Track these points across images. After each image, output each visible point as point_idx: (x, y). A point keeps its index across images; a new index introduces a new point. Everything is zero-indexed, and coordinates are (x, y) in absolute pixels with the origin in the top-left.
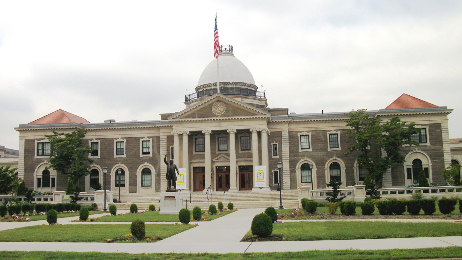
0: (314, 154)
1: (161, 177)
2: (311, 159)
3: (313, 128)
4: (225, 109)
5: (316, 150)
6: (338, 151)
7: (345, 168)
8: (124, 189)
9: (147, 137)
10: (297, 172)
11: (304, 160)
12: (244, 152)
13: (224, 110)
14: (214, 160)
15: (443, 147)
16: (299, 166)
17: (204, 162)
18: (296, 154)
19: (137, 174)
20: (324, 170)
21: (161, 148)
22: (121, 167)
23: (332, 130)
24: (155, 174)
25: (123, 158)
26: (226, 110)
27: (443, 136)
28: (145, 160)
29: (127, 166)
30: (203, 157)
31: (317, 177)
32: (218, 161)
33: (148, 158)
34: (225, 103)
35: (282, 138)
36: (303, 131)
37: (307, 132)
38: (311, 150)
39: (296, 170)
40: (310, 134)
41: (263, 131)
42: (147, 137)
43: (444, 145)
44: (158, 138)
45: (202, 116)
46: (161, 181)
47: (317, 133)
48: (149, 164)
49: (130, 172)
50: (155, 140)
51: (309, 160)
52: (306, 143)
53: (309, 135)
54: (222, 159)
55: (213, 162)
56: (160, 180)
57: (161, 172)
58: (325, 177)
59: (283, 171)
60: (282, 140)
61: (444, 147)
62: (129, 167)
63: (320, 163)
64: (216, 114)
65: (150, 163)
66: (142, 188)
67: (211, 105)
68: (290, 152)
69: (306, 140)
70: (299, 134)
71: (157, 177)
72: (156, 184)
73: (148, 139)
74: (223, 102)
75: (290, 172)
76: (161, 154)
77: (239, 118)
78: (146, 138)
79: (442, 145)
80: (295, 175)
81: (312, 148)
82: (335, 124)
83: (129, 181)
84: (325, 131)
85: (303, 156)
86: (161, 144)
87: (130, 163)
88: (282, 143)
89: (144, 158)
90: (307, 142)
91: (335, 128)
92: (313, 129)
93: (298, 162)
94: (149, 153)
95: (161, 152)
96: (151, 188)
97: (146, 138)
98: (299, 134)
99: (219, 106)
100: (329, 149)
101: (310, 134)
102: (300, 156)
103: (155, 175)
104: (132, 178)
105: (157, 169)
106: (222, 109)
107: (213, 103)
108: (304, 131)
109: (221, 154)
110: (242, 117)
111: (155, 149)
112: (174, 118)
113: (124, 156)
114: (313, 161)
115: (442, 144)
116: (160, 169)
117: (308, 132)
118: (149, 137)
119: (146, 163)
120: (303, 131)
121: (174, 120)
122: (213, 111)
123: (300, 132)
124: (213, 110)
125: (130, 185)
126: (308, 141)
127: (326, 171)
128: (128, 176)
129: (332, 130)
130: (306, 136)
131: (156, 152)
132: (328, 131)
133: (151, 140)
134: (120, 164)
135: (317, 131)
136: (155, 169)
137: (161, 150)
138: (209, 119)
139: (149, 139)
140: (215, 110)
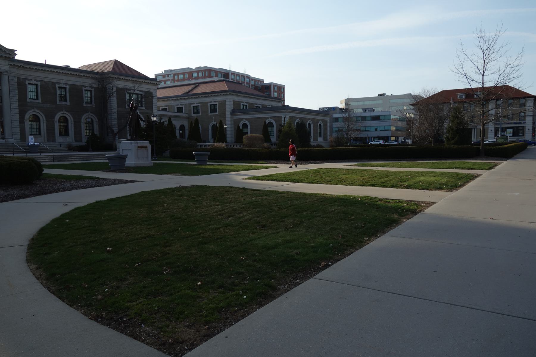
3: (42, 78)
6: (66, 105)
7: (74, 123)
15: (153, 112)
16: (27, 116)
20: (54, 124)
23: (61, 83)
27: (154, 103)
31: (47, 130)
36: (32, 80)
38: (40, 101)
39: (25, 121)
40: (39, 84)
43: (154, 110)
51: (38, 112)
52: (33, 93)
58: (54, 130)
61: (154, 112)
63: (50, 117)
69: (33, 89)
70: (27, 82)
75: (20, 123)
79: (153, 110)
81: (41, 99)
82: (64, 77)
84: (54, 84)
91: (64, 82)
93: (26, 112)
100: (58, 103)
101: (39, 84)
114: (43, 113)
115: (153, 109)
117: (37, 81)
120: (32, 80)
126: (35, 91)
127: (56, 124)
129: (61, 83)
130: (33, 86)
132: (58, 84)
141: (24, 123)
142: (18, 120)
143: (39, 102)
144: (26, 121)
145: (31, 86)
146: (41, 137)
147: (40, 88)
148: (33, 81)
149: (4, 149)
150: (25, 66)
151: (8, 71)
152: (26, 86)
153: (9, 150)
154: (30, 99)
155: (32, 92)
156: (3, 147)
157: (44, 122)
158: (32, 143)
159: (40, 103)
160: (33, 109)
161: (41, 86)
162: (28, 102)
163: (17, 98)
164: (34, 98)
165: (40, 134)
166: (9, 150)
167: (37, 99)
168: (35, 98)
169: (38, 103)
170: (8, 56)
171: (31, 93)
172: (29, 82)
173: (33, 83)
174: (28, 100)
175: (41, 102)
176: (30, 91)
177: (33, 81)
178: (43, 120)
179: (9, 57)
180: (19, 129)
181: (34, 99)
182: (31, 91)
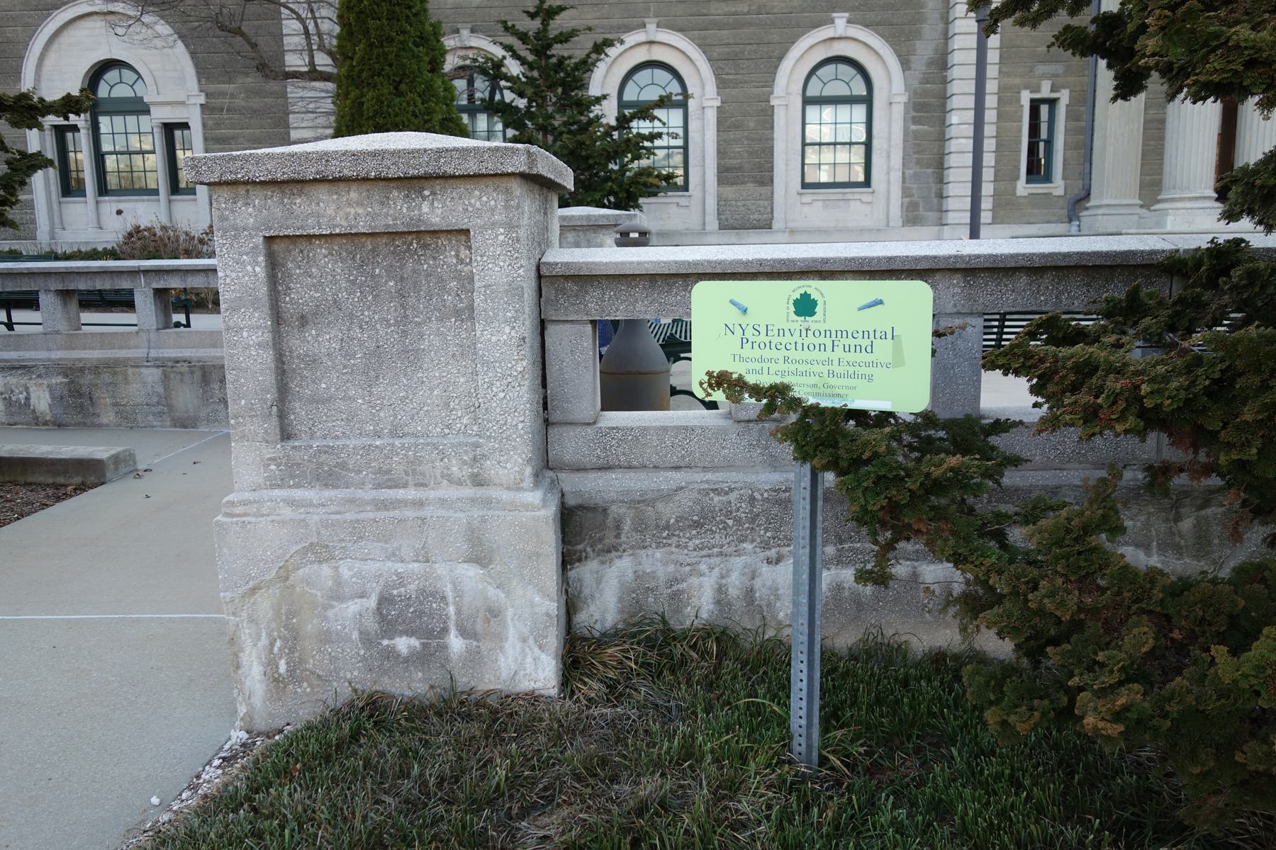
8: (683, 201)
22: (659, 54)
24: (904, 99)
29: (704, 47)
49: (722, 84)
62: (716, 52)
65: (866, 26)
71: (916, 121)
83: (721, 153)
87: (721, 27)
96: (866, 198)
104: (737, 126)
125: (726, 174)
128: (711, 116)
134: (653, 31)
136: (905, 64)
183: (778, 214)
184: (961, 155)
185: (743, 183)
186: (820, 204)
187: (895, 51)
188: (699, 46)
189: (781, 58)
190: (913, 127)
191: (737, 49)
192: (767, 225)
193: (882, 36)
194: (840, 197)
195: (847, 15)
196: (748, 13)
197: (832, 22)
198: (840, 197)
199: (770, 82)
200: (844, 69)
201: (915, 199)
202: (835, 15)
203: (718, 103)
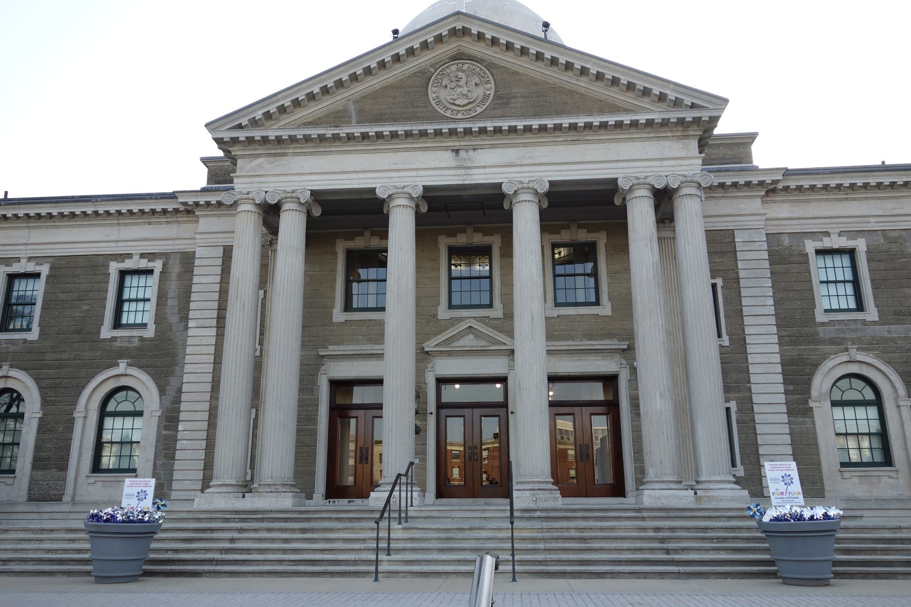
0: (889, 332)
1: (180, 428)
2: (878, 357)
3: (873, 220)
4: (492, 92)
5: (896, 313)
8: (10, 481)
9: (142, 256)
10: (816, 413)
11: (845, 358)
12: (571, 311)
13: (486, 97)
14: (429, 346)
16: (821, 383)
17: (380, 356)
18: (806, 329)
19: (76, 415)
21: (193, 297)
24: (159, 413)
25: (25, 341)
26: (497, 97)
28: (122, 353)
29: (37, 380)
30: (377, 333)
32: (449, 354)
33: (136, 343)
34: (491, 66)
35: (739, 256)
36: (827, 234)
37: (845, 238)
38: (872, 313)
39: (811, 404)
41: (685, 191)
42: (142, 256)
44: (188, 260)
45: (379, 119)
46: (179, 445)
47: (894, 241)
48: (132, 371)
49: (45, 402)
50: (175, 268)
52: (841, 287)
53: (851, 252)
54: (469, 341)
55: (423, 356)
56: (175, 440)
57: (183, 406)
59: (756, 408)
60: (740, 265)
64: (448, 114)
65: (140, 368)
66: (92, 480)
67: (424, 77)
68: (782, 321)
69: (839, 272)
70: (810, 246)
72: (159, 463)
73: (144, 264)
74: (481, 61)
75: (789, 413)
76: (191, 324)
77: (566, 122)
78: (136, 258)
80: (810, 425)
81: (876, 306)
83: (38, 448)
85: (839, 343)
86: (196, 280)
87: (50, 367)
88: (737, 279)
89: (118, 344)
90: (844, 282)
92: (873, 225)
93: (816, 366)
94: (144, 326)
95: (192, 315)
97: (136, 258)
98: (810, 246)
99: (460, 74)
101: (861, 245)
102: (823, 342)
103: (157, 419)
105: (171, 391)
106: (478, 93)
107: (435, 66)
108: (830, 231)
109: (462, 319)
110: (581, 121)
111: (172, 302)
112: (240, 127)
113: (34, 335)
114: (889, 363)
116: (180, 391)
118: (151, 256)
119: (123, 366)
120: (827, 234)
121: (242, 135)
122: (433, 103)
123: (812, 235)
124: (431, 96)
125: (38, 463)
126: (849, 276)
128: (35, 424)
131: (174, 319)
133: (158, 266)
135: (890, 234)
136: (162, 391)
137: (192, 306)
138: (416, 128)
139: (151, 265)
140: (442, 98)
141: (808, 412)
142: (782, 398)
143: (868, 319)
144: (817, 404)
145: (829, 261)
146: (893, 474)
147: (869, 260)
148: (834, 237)
149: (638, 545)
150: (793, 184)
151: (699, 180)
152: (807, 262)
153: (667, 551)
154: (826, 311)
155: (836, 282)
156: (644, 529)
157: (901, 403)
158: (785, 510)
159: (874, 323)
160: (847, 350)
161: (869, 252)
162: (823, 324)
163: (772, 310)
164: (844, 306)
165: (888, 461)
166: (667, 551)
167: (860, 307)
168: (853, 305)
169: (864, 323)
170: (689, 115)
171: (832, 287)
172: (819, 245)
173: (836, 246)
174: (820, 317)
175: (876, 318)
176: (827, 282)
177: (834, 237)
178: (897, 398)
179: (697, 121)
180: (788, 439)
181: (848, 310)
182: (832, 278)
183: (69, 491)
184: (183, 451)
185: (49, 469)
186: (101, 483)
187: (156, 383)
188: (35, 379)
189: (84, 387)
190: (164, 432)
191: (58, 381)
192: (60, 500)
193: (149, 374)
194: (114, 479)
195: (126, 361)
196: (68, 359)
197: (117, 365)
198: (114, 479)
199: (75, 403)
200: (122, 394)
201: (162, 481)
202: (119, 361)
203: (40, 415)
